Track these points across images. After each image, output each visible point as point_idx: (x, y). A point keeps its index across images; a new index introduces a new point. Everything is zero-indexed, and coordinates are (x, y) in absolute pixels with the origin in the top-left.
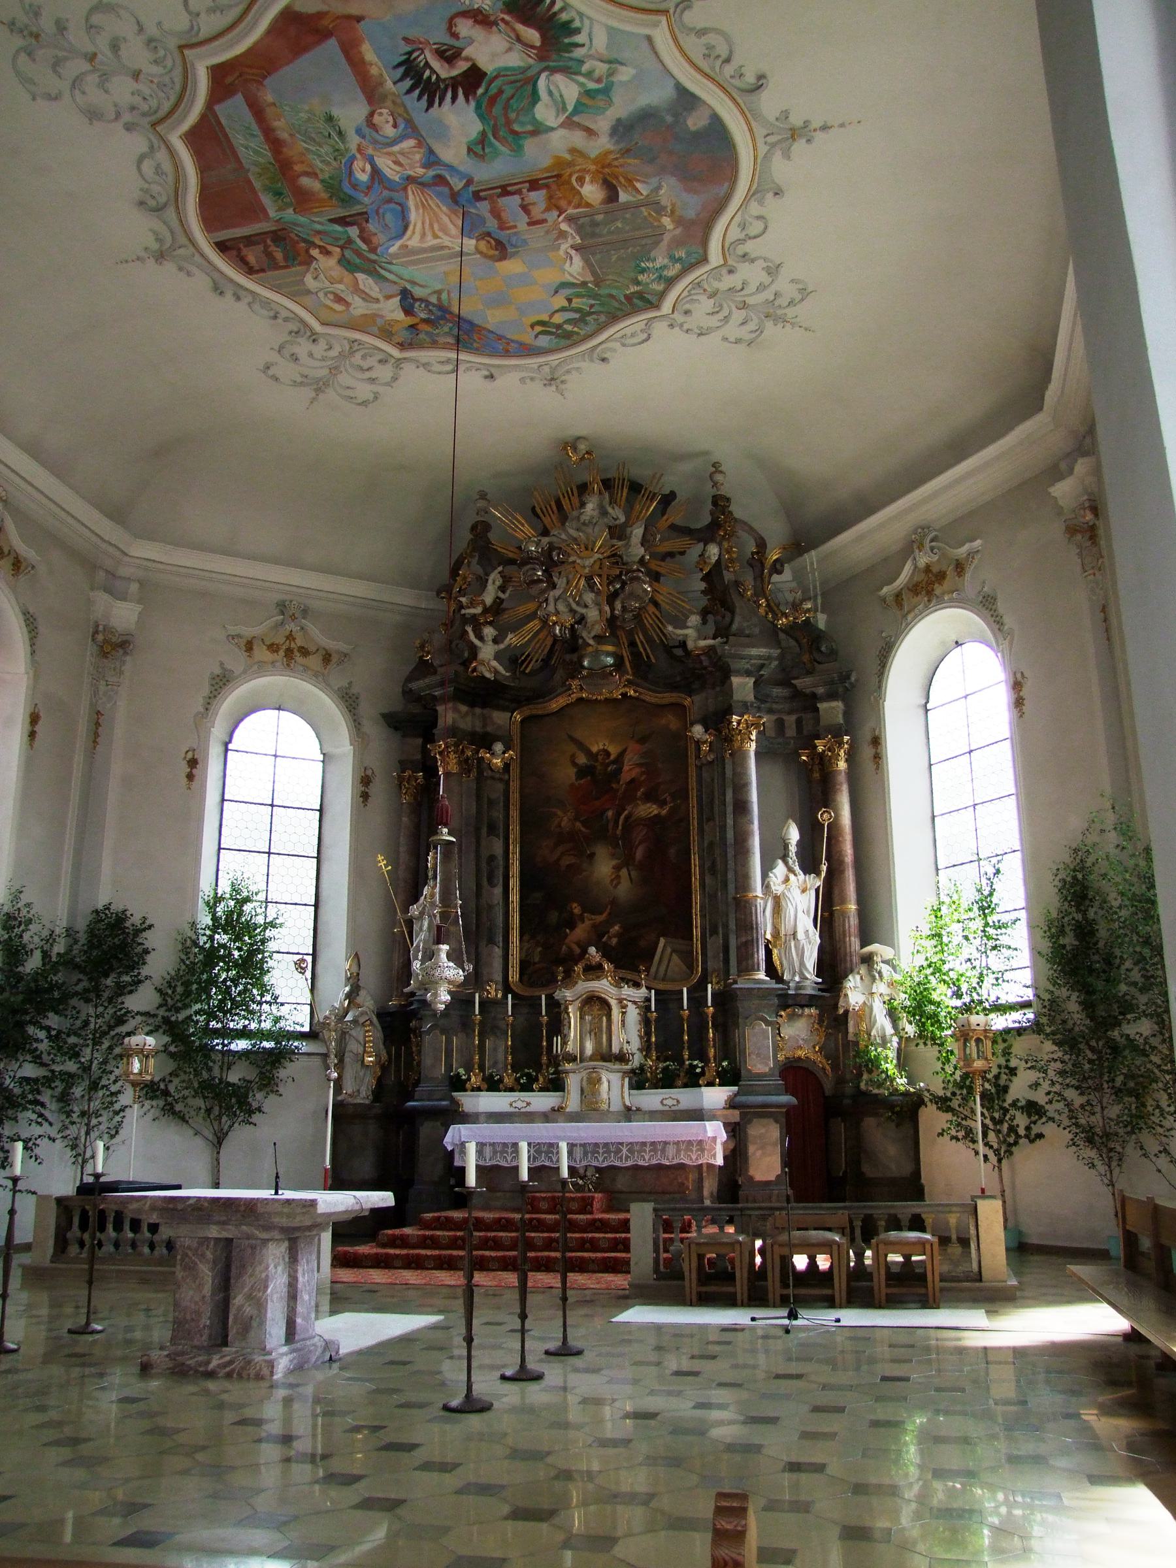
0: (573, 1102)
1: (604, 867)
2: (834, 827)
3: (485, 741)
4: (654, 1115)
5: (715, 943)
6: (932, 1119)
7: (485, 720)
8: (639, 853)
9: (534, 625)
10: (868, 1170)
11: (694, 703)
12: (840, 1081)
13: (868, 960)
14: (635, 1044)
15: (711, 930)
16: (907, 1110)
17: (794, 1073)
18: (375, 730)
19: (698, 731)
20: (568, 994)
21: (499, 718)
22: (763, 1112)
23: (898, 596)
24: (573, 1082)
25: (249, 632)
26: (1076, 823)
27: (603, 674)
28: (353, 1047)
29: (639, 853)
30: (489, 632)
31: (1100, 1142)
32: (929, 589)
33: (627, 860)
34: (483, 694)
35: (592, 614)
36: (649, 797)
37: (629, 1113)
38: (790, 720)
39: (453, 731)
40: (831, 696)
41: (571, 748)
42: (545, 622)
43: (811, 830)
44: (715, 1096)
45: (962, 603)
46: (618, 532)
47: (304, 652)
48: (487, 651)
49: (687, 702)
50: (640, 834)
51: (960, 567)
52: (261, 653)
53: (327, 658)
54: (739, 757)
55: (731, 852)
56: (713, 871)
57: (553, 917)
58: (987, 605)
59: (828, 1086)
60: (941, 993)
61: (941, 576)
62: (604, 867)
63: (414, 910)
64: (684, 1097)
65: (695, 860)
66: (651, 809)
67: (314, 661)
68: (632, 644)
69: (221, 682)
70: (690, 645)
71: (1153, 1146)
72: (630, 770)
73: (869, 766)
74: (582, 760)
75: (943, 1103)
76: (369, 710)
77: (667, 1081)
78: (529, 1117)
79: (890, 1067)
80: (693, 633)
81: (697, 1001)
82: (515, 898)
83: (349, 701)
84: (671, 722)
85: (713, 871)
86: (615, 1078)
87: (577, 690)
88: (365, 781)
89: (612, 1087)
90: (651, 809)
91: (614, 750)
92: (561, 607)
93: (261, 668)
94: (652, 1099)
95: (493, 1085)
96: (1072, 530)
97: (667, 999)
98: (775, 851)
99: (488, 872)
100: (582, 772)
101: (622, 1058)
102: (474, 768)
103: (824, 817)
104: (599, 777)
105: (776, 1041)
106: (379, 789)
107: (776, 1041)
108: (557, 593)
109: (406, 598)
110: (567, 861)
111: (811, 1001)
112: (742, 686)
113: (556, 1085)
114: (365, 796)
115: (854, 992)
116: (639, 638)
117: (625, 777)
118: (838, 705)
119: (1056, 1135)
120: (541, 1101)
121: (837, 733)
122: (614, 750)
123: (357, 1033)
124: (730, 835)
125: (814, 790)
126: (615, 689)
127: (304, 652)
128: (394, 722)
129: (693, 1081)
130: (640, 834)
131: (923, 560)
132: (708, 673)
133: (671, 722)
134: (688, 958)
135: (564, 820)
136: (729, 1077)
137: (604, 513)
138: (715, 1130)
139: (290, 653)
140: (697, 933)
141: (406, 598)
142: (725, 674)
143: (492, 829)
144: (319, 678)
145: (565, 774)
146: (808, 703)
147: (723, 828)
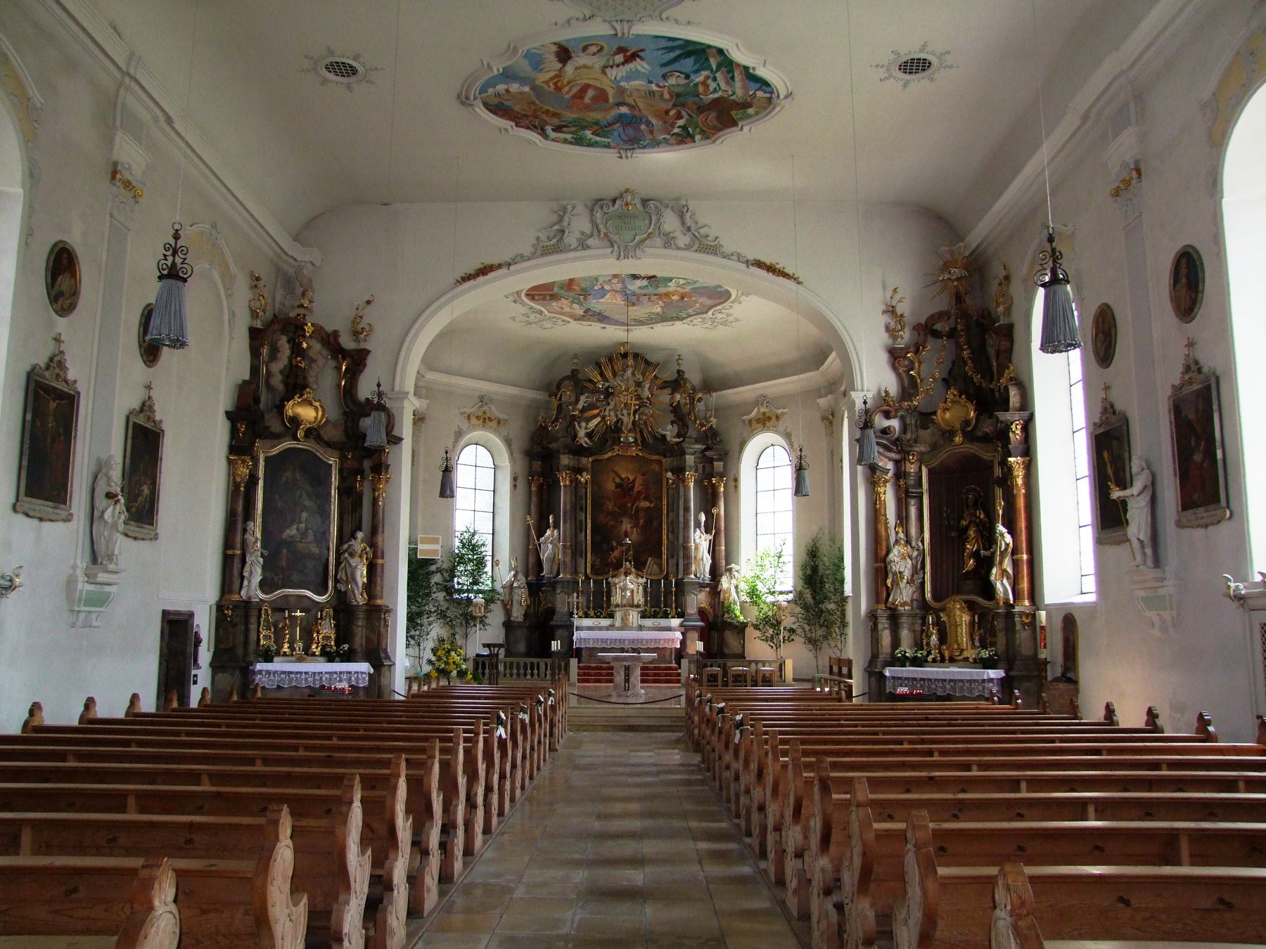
0: (618, 623)
1: (626, 525)
2: (718, 515)
3: (578, 470)
4: (650, 629)
5: (672, 562)
6: (751, 633)
7: (579, 462)
8: (641, 522)
9: (599, 419)
10: (726, 651)
11: (667, 462)
12: (716, 616)
13: (730, 570)
14: (642, 601)
15: (671, 555)
16: (741, 629)
17: (701, 612)
18: (519, 456)
19: (669, 475)
20: (616, 580)
21: (584, 460)
22: (694, 628)
23: (750, 421)
24: (618, 615)
25: (468, 411)
26: (814, 528)
27: (629, 445)
28: (516, 598)
29: (641, 522)
30: (583, 424)
31: (813, 642)
32: (764, 422)
33: (636, 525)
34: (578, 451)
35: (625, 419)
36: (646, 499)
37: (641, 628)
38: (700, 466)
39: (568, 468)
40: (719, 460)
41: (612, 475)
42: (603, 418)
43: (709, 515)
44: (675, 622)
45: (777, 432)
46: (639, 384)
47: (490, 419)
48: (582, 433)
49: (664, 460)
50: (642, 514)
51: (778, 418)
52: (474, 421)
53: (499, 422)
54: (686, 488)
55: (681, 526)
56: (673, 532)
57: (605, 547)
58: (787, 436)
59: (711, 619)
60: (760, 587)
61: (769, 419)
62: (626, 525)
63: (542, 539)
64: (663, 622)
65: (665, 526)
66: (647, 504)
67: (494, 424)
68: (641, 432)
69: (459, 434)
70: (668, 438)
71: (833, 644)
72: (638, 487)
73: (732, 490)
74: (618, 480)
75: (756, 627)
76: (515, 446)
77: (655, 616)
78: (600, 628)
79: (738, 613)
80: (670, 432)
81: (668, 584)
82: (589, 538)
83: (508, 442)
84: (655, 467)
85: (673, 532)
86: (635, 614)
87: (617, 451)
88: (515, 479)
89: (634, 617)
90: (647, 504)
91: (631, 478)
92: (612, 414)
93: (474, 428)
94: (649, 622)
95: (587, 616)
96: (824, 418)
97: (655, 583)
98: (698, 525)
99: (578, 527)
100: (618, 486)
101: (638, 606)
102: (575, 484)
103: (714, 511)
104: (625, 488)
105: (697, 600)
106: (520, 482)
107: (697, 600)
108: (611, 407)
109: (531, 394)
110: (611, 523)
111: (707, 585)
112: (690, 459)
113: (611, 616)
114: (515, 486)
115: (725, 583)
116: (645, 432)
117: (636, 490)
118: (721, 463)
119: (799, 640)
120: (605, 622)
121: (721, 476)
122: (631, 478)
123: (518, 591)
124: (681, 519)
125: (709, 499)
126: (633, 451)
127: (490, 419)
128: (530, 454)
129: (666, 616)
130: (642, 514)
131: (762, 410)
132: (678, 452)
133: (655, 467)
134: (660, 566)
135: (610, 506)
136: (681, 615)
137: (633, 374)
138: (678, 635)
139: (486, 421)
140: (665, 557)
141: (531, 394)
142: (683, 453)
143: (581, 509)
144: (496, 432)
145: (611, 486)
146: (711, 461)
147: (678, 515)
